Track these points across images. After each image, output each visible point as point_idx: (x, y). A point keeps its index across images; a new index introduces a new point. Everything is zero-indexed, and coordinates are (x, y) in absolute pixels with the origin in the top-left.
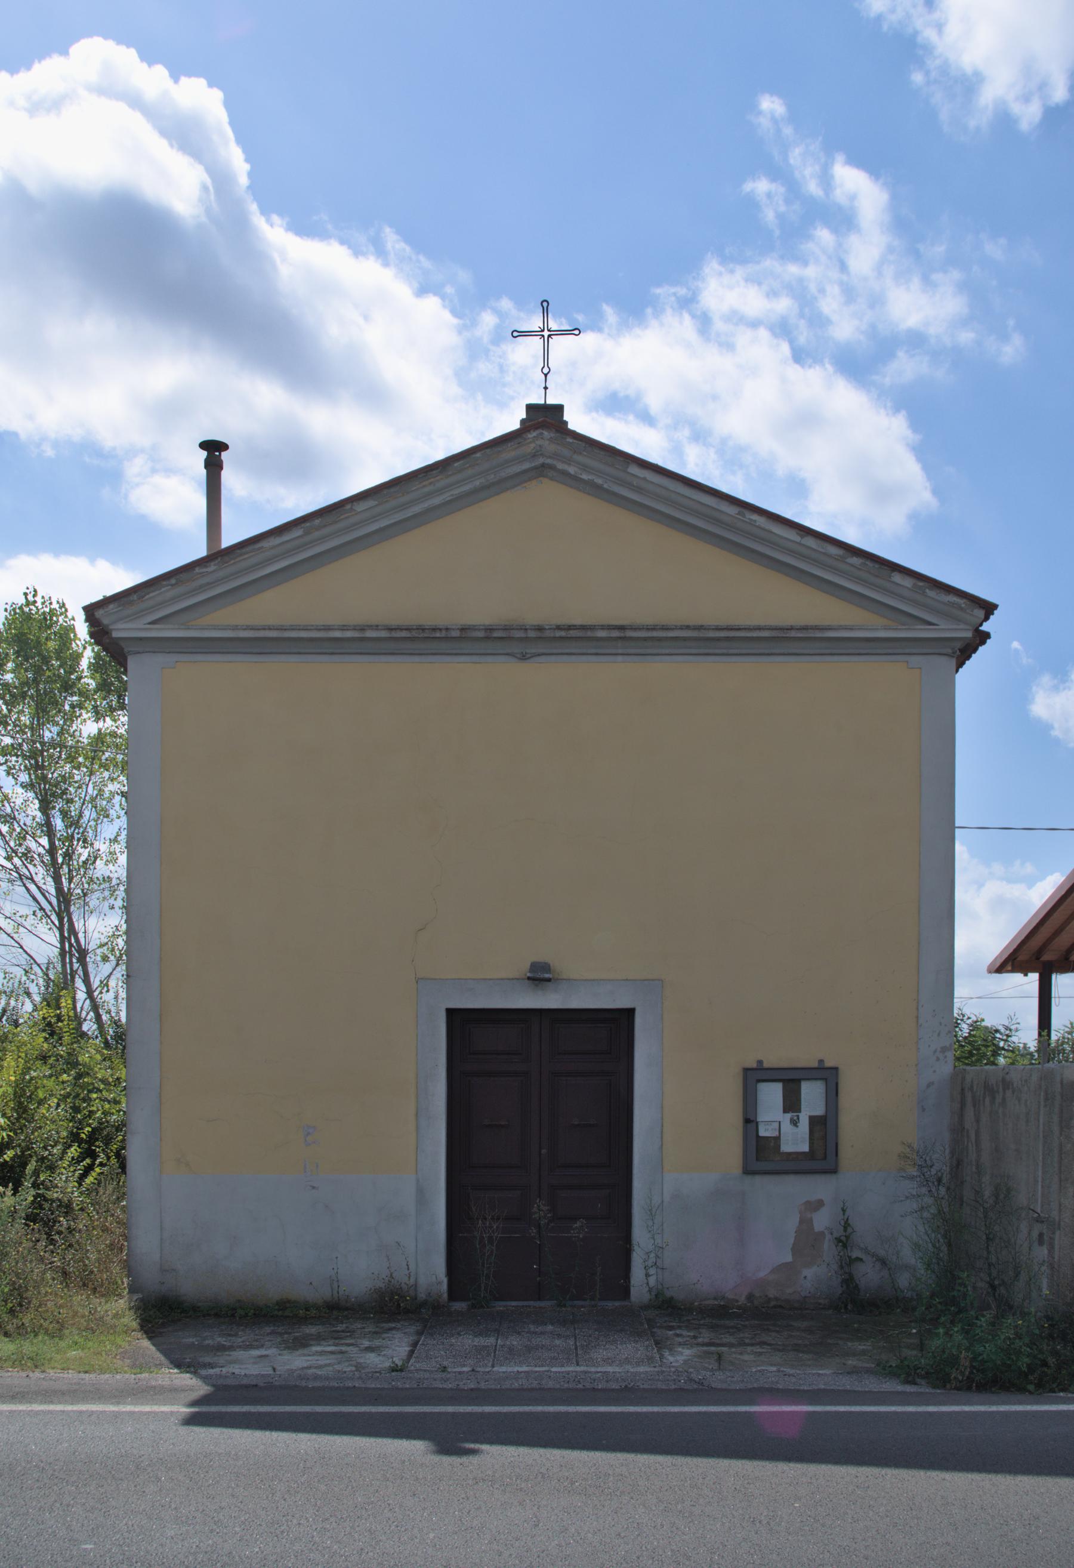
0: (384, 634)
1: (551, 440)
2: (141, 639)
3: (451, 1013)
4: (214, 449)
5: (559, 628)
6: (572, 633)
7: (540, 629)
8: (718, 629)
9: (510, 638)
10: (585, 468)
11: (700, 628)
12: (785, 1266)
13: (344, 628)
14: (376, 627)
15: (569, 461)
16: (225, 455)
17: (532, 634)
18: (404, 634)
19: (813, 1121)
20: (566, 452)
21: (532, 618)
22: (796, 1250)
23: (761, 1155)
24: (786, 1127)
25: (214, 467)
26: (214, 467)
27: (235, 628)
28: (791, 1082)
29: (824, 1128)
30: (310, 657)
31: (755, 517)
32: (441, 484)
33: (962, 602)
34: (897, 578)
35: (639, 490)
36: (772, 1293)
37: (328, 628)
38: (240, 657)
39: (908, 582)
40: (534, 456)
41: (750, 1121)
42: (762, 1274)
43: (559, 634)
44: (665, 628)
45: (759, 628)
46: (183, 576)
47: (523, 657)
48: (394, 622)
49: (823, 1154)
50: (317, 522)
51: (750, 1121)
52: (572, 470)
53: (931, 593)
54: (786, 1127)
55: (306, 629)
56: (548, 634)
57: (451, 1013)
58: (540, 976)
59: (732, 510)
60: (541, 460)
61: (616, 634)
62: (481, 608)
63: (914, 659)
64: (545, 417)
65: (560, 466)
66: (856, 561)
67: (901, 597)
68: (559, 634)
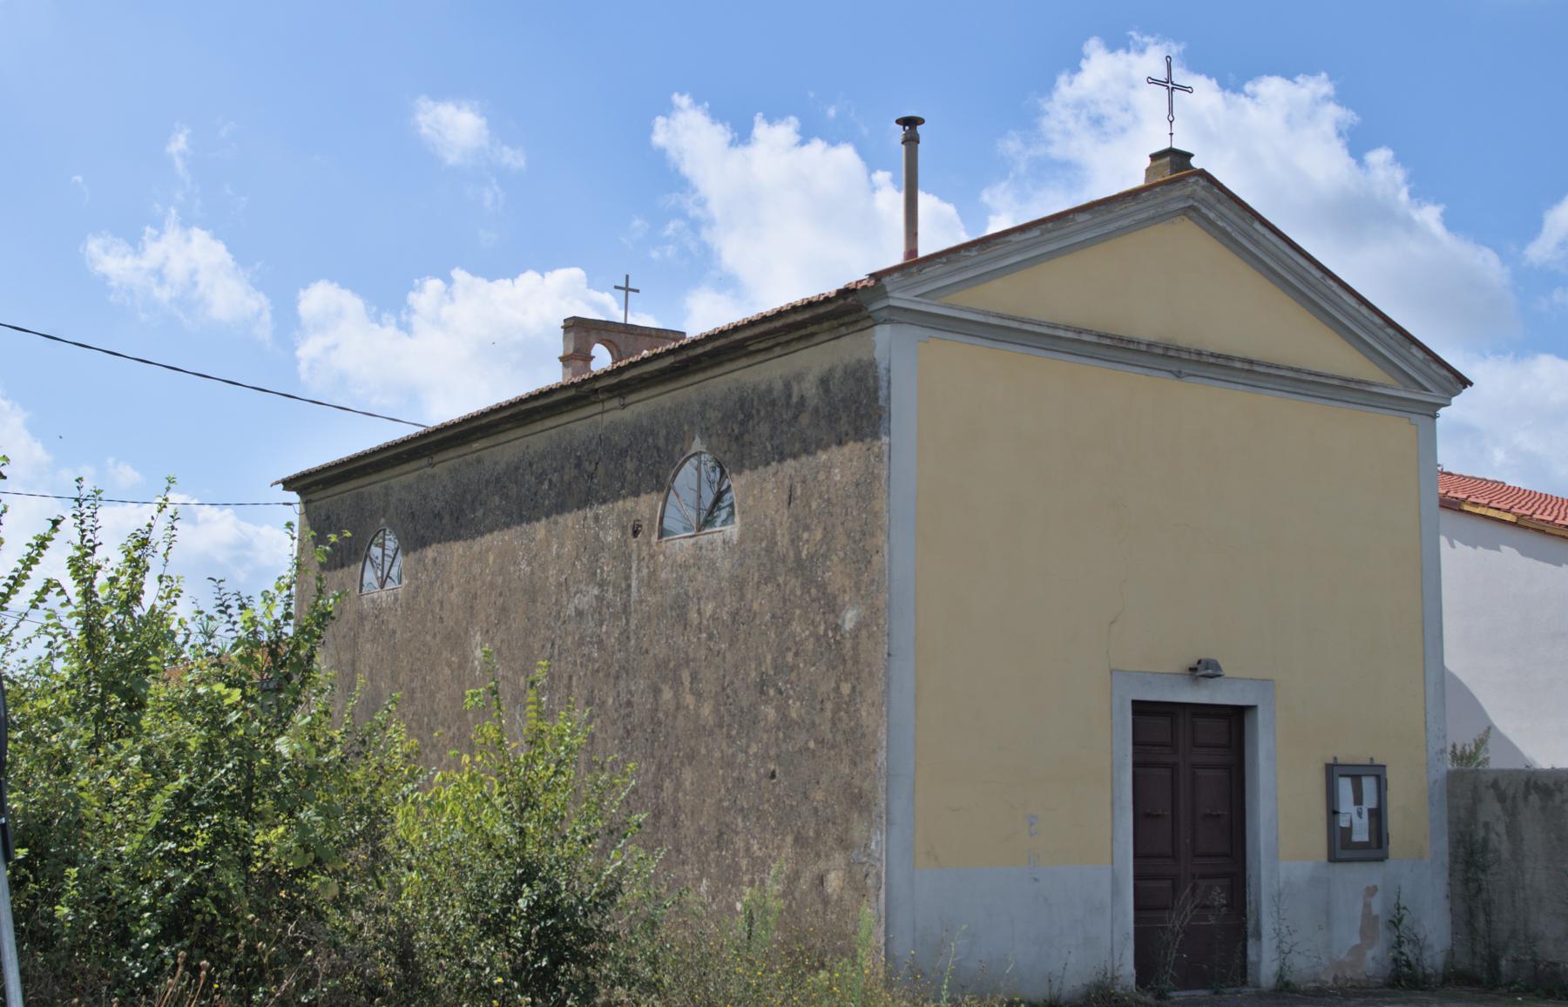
0: (1094, 339)
1: (1203, 188)
2: (906, 310)
3: (1134, 702)
4: (910, 123)
5: (1212, 355)
6: (1220, 361)
7: (1199, 353)
8: (1310, 373)
9: (1179, 358)
10: (1222, 216)
11: (1298, 371)
12: (1357, 946)
13: (1067, 328)
14: (1090, 332)
15: (1210, 207)
16: (920, 129)
17: (1143, 348)
18: (1108, 342)
19: (1370, 811)
20: (1212, 200)
21: (1182, 341)
22: (1363, 933)
23: (1341, 847)
24: (1356, 819)
25: (911, 141)
26: (911, 141)
27: (987, 314)
28: (1356, 774)
29: (1378, 816)
30: (1032, 350)
31: (1331, 282)
32: (1132, 209)
33: (1450, 376)
34: (1414, 350)
35: (1256, 243)
36: (1349, 974)
37: (1056, 327)
38: (978, 341)
39: (1420, 355)
40: (1188, 197)
41: (1333, 812)
42: (1342, 956)
43: (1212, 360)
44: (1278, 367)
45: (1333, 377)
46: (952, 256)
47: (1178, 375)
48: (1102, 330)
49: (1377, 847)
50: (1050, 225)
51: (1333, 812)
52: (1211, 215)
53: (1434, 366)
54: (1356, 819)
55: (1040, 324)
56: (1204, 359)
57: (1134, 702)
58: (1203, 671)
59: (1318, 274)
60: (1191, 202)
61: (1246, 366)
62: (1147, 325)
63: (1415, 418)
64: (1174, 161)
65: (1204, 210)
66: (1390, 331)
67: (1413, 366)
68: (1212, 360)
